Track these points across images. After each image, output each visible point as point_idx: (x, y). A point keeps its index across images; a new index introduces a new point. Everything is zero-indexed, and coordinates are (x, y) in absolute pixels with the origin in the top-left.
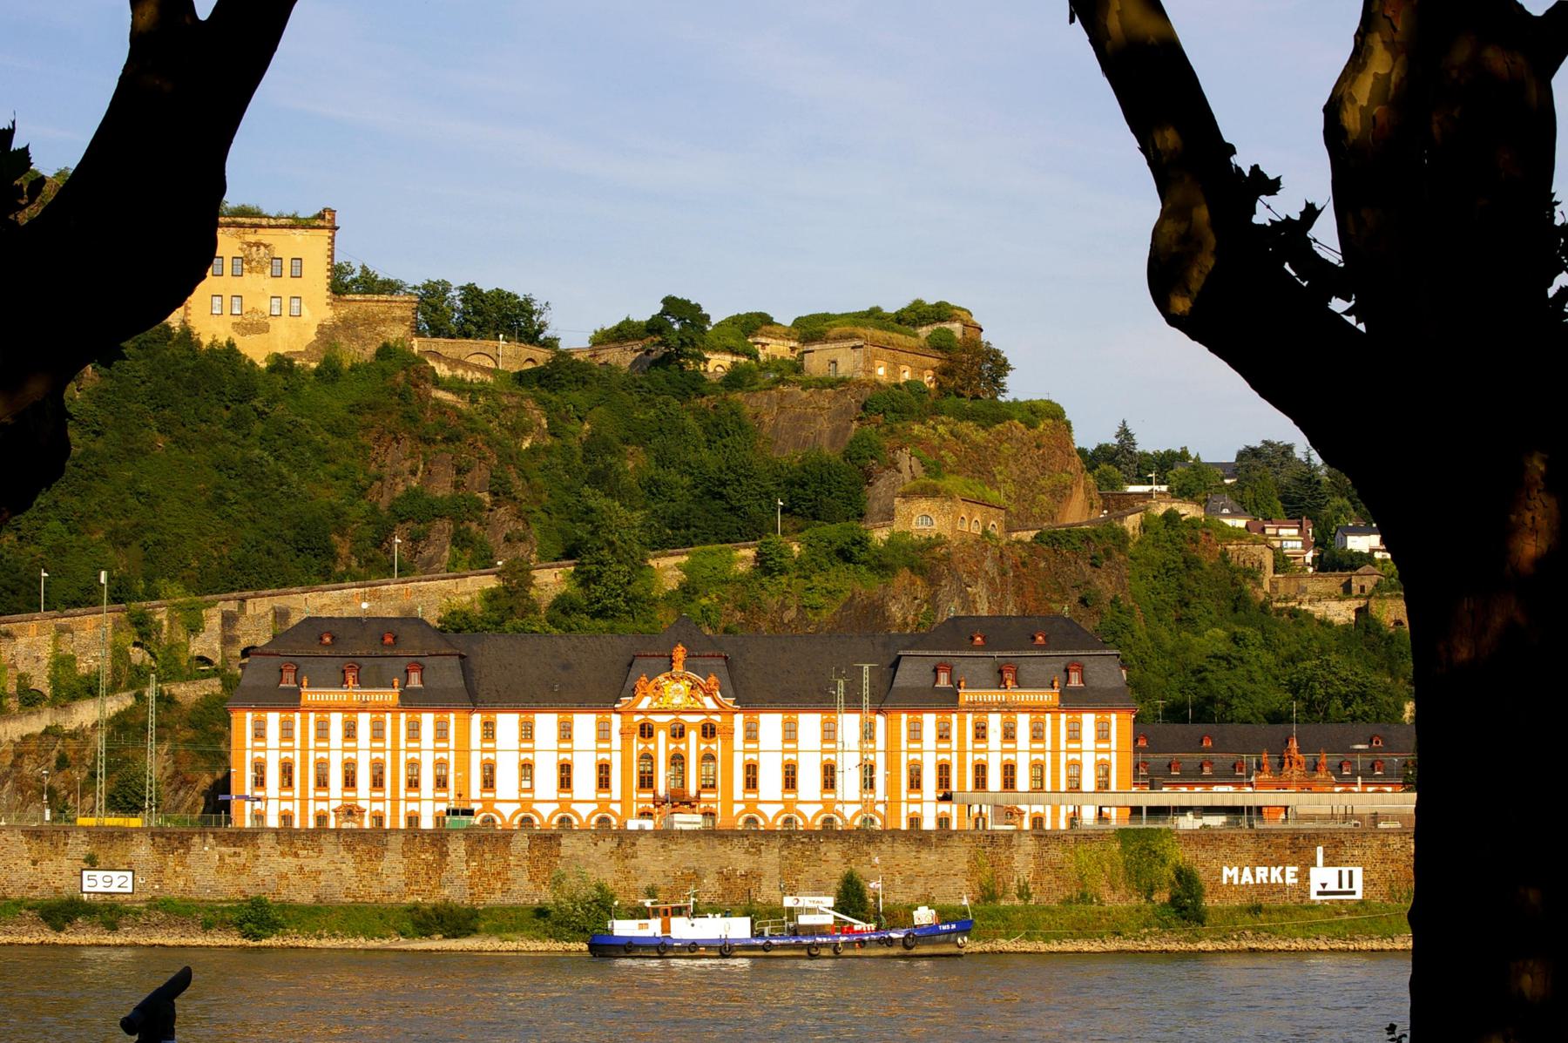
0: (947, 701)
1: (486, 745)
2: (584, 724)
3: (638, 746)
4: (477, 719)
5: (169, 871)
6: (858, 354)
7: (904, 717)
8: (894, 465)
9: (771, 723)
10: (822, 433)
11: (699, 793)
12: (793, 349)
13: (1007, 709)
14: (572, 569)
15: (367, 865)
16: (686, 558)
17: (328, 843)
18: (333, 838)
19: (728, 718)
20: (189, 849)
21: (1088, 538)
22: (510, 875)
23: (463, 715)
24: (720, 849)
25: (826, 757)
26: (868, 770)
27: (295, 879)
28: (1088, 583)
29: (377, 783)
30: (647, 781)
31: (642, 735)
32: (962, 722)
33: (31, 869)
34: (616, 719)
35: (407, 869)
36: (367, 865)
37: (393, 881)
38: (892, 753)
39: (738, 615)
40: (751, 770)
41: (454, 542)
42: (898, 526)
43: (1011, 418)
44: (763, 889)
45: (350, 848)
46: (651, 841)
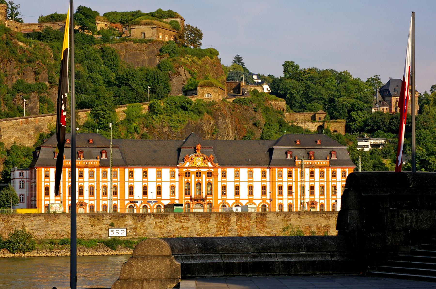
0: (291, 164)
1: (130, 180)
2: (166, 172)
3: (185, 180)
4: (127, 170)
5: (138, 228)
6: (154, 30)
7: (277, 169)
8: (178, 73)
9: (230, 172)
10: (146, 61)
11: (206, 196)
12: (106, 25)
13: (312, 167)
14: (89, 112)
15: (204, 225)
16: (126, 108)
17: (191, 217)
18: (193, 216)
19: (216, 170)
20: (145, 220)
21: (251, 101)
22: (250, 227)
23: (122, 169)
24: (317, 218)
25: (249, 183)
26: (264, 188)
27: (180, 230)
28: (254, 118)
29: (91, 193)
30: (188, 192)
31: (186, 176)
32: (296, 171)
33: (91, 229)
34: (177, 170)
35: (217, 226)
36: (204, 225)
37: (213, 230)
38: (272, 181)
39: (146, 129)
40: (224, 188)
41: (40, 101)
42: (199, 97)
43: (206, 55)
44: (331, 231)
45: (199, 219)
46: (295, 216)
